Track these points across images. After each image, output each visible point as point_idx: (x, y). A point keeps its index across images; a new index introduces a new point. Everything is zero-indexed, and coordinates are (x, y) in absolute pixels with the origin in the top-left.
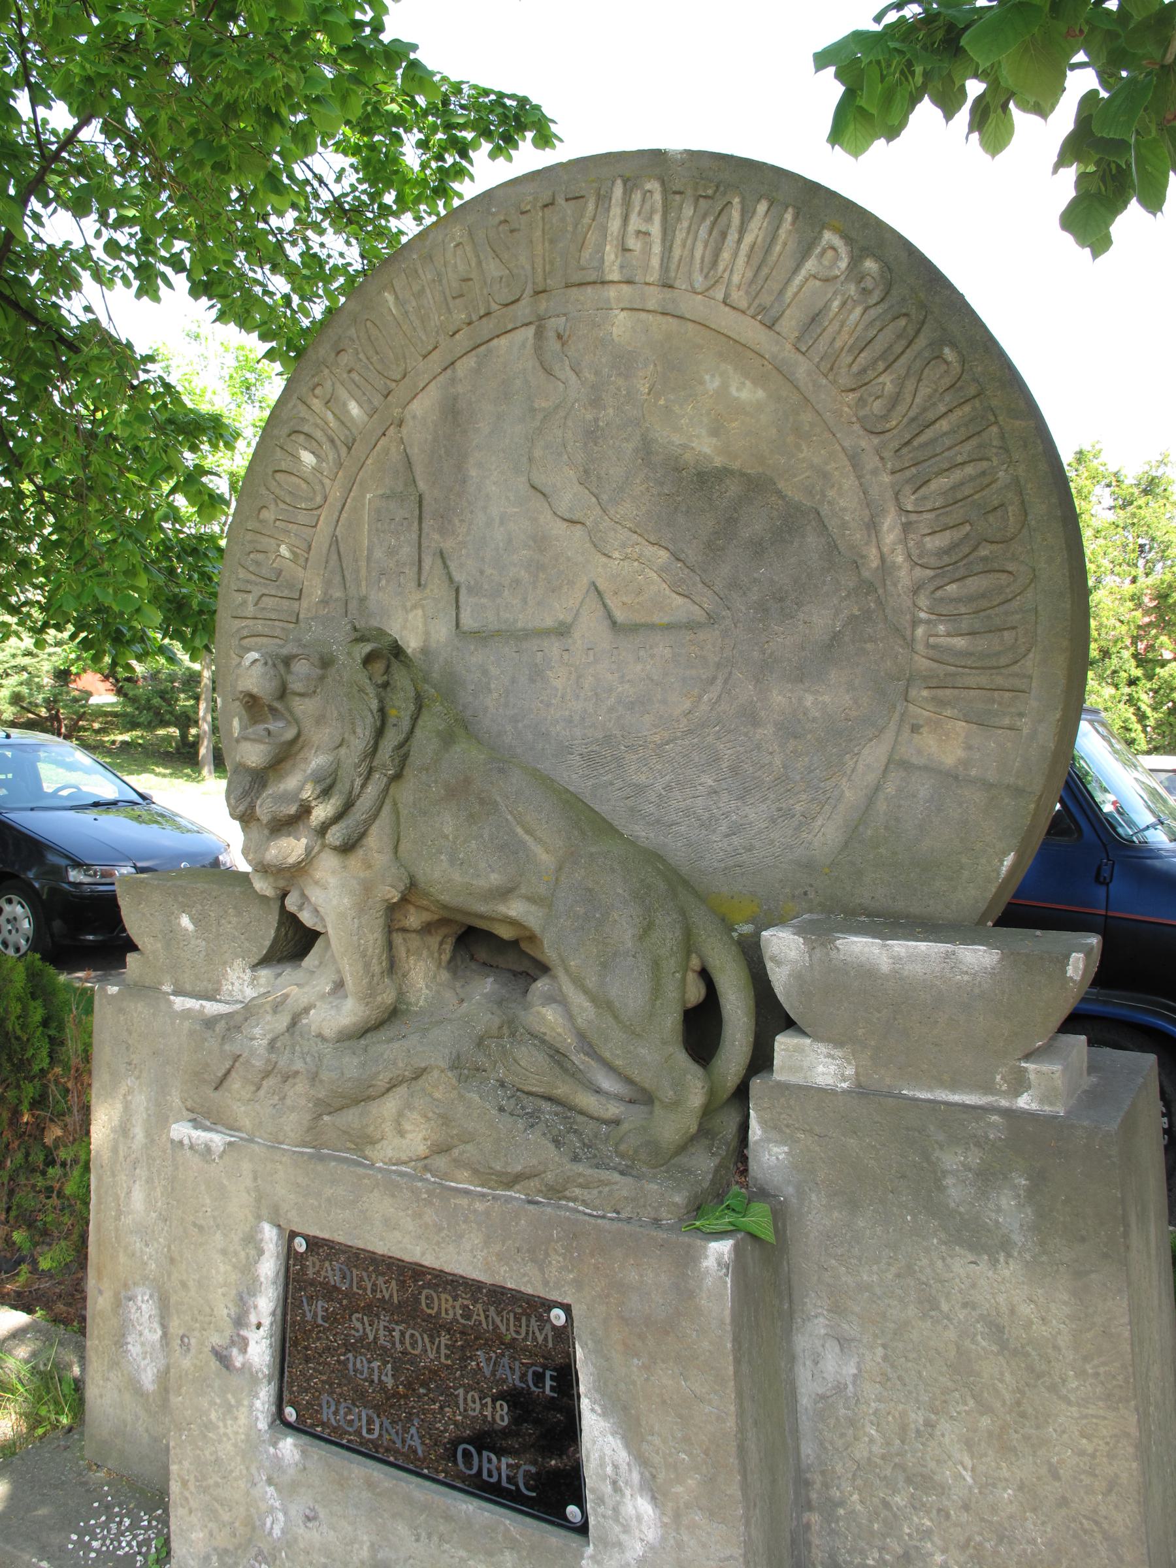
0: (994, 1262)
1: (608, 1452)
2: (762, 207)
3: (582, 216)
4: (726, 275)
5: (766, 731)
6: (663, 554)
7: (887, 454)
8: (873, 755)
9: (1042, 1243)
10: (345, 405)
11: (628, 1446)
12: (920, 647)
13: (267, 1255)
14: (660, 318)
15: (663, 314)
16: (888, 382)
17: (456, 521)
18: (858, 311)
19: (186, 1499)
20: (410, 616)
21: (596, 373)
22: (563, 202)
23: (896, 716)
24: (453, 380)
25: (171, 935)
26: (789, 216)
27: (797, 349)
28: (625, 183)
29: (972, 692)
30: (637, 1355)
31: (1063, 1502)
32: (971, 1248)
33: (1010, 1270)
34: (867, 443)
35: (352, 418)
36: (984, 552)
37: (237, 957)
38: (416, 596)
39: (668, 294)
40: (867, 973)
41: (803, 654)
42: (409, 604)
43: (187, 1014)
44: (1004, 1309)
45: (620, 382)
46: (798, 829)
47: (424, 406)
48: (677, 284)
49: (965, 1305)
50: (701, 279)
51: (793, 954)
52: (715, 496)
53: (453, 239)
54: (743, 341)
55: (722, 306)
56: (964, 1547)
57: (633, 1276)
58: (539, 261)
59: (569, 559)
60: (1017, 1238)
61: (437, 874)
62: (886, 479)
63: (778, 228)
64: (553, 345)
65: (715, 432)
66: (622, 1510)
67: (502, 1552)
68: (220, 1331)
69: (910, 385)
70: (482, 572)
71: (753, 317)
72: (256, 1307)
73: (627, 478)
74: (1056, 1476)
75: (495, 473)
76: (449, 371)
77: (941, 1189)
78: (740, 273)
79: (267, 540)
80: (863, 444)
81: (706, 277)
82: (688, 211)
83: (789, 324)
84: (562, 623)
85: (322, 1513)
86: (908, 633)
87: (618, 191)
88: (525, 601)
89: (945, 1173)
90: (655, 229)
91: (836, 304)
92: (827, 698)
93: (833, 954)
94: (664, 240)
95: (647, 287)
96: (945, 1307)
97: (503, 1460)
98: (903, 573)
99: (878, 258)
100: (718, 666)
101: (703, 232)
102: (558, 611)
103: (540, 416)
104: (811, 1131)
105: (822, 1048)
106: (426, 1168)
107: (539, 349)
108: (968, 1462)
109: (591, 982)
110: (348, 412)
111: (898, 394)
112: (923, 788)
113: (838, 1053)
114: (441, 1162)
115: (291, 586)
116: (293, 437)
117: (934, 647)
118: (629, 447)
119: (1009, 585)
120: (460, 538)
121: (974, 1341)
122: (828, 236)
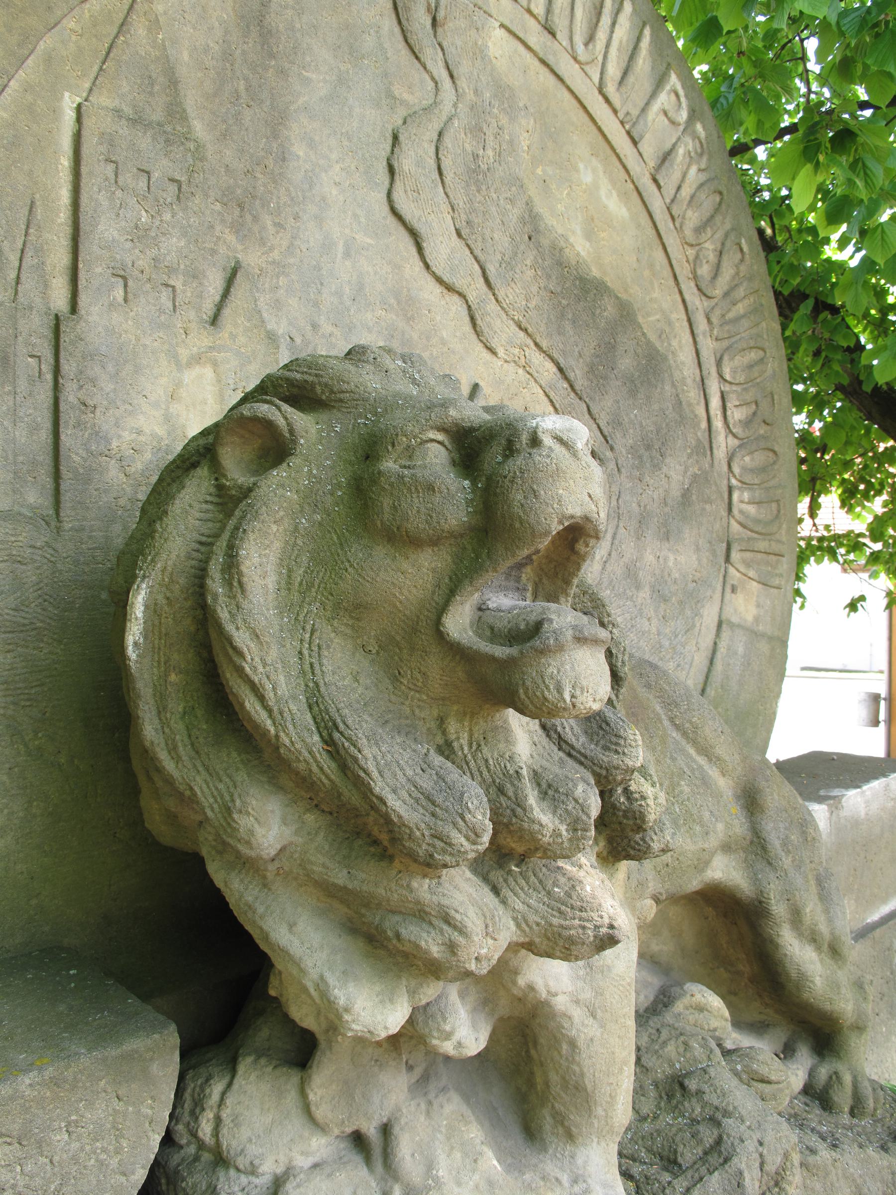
4: (600, 58)
5: (644, 594)
7: (714, 320)
8: (709, 615)
12: (735, 511)
14: (537, 63)
15: (543, 62)
17: (268, 221)
18: (693, 170)
20: (188, 376)
21: (476, 91)
23: (721, 579)
27: (655, 181)
29: (759, 556)
38: (200, 340)
41: (667, 509)
42: (184, 353)
45: (504, 121)
48: (559, 35)
50: (582, 47)
52: (598, 311)
54: (613, 143)
55: (596, 92)
59: (443, 342)
63: (639, 39)
65: (589, 235)
70: (315, 327)
71: (622, 123)
75: (337, 168)
83: (648, 147)
103: (402, 112)
118: (515, 213)
119: (774, 463)
120: (275, 255)
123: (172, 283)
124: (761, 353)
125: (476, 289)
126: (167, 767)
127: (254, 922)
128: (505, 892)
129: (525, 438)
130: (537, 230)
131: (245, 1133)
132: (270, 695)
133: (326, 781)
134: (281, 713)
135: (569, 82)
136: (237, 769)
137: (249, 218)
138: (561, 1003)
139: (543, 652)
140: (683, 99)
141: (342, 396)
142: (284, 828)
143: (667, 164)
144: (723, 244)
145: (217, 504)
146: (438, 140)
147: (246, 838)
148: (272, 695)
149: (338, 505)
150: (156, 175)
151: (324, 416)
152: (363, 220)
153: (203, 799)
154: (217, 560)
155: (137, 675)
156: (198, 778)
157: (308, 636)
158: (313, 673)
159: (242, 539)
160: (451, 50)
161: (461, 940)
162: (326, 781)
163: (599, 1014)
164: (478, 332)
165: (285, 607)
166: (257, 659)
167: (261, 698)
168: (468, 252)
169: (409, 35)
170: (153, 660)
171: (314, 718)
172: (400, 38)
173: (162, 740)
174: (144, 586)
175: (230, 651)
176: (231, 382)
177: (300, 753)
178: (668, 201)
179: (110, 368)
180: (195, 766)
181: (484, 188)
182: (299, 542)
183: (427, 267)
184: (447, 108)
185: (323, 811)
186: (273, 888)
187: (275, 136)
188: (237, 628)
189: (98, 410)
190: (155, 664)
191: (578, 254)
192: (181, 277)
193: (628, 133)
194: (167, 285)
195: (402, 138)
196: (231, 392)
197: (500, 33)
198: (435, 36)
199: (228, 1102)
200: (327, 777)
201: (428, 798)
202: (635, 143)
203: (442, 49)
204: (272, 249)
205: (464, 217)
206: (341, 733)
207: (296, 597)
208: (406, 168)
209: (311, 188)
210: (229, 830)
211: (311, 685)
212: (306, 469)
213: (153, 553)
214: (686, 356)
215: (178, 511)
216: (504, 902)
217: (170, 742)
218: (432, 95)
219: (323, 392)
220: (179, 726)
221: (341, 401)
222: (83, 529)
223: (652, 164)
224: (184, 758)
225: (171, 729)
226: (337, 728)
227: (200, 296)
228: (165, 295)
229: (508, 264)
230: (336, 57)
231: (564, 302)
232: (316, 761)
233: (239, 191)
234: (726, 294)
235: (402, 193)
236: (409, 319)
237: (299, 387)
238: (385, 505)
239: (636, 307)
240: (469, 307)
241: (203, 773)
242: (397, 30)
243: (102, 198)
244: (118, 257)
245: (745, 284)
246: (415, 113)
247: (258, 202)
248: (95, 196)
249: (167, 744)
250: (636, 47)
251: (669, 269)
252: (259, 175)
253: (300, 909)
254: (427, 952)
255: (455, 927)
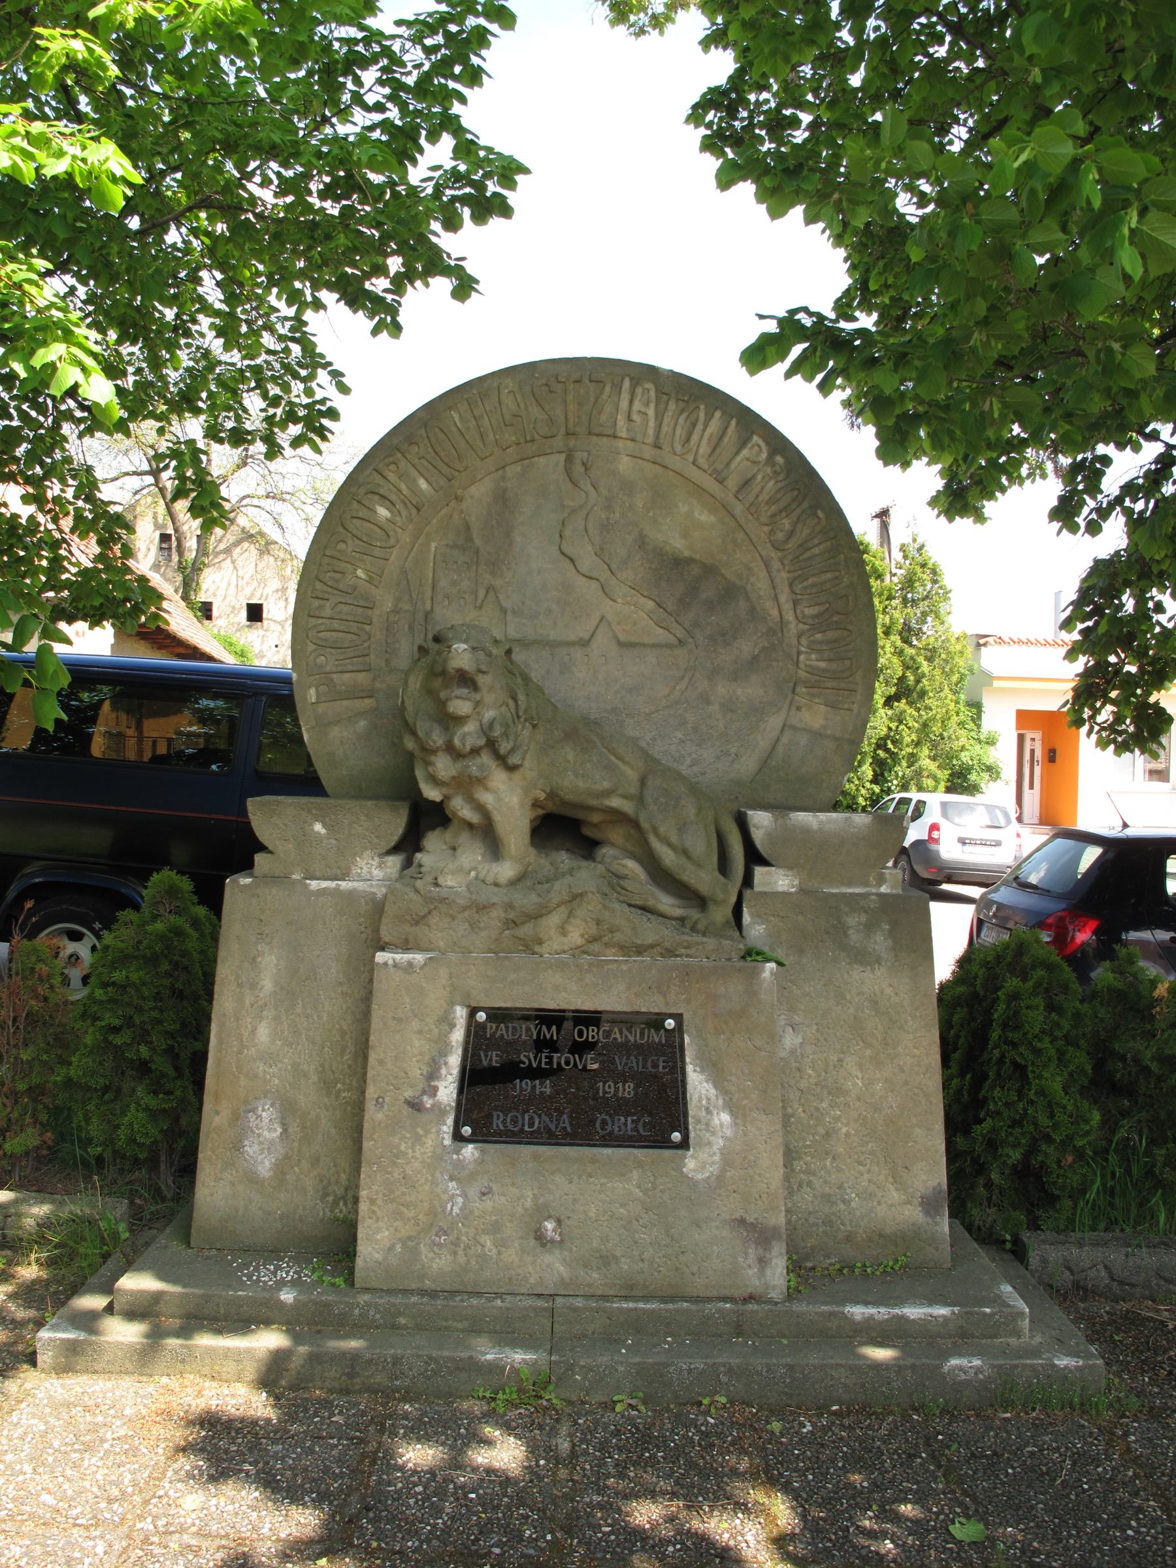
0: (873, 970)
1: (704, 1092)
2: (718, 414)
3: (601, 394)
6: (651, 604)
7: (786, 562)
8: (774, 723)
9: (896, 956)
10: (415, 480)
11: (716, 1087)
12: (802, 665)
13: (458, 1026)
16: (786, 524)
18: (772, 483)
19: (374, 1212)
22: (587, 382)
23: (788, 702)
24: (503, 478)
25: (305, 839)
26: (733, 422)
28: (632, 379)
30: (724, 1033)
31: (906, 1083)
32: (862, 963)
33: (880, 972)
34: (774, 555)
35: (421, 490)
36: (835, 618)
37: (366, 849)
39: (658, 452)
40: (806, 830)
43: (323, 892)
44: (878, 992)
46: (733, 762)
47: (480, 491)
49: (859, 994)
51: (766, 823)
53: (507, 387)
56: (856, 1121)
57: (722, 990)
58: (570, 416)
60: (884, 955)
61: (566, 783)
62: (784, 575)
63: (726, 428)
64: (578, 469)
65: (685, 536)
66: (712, 1123)
67: (631, 1171)
68: (412, 1086)
69: (799, 526)
70: (523, 603)
72: (446, 1064)
74: (902, 1071)
76: (500, 472)
77: (846, 936)
78: (704, 449)
79: (343, 564)
80: (773, 555)
81: (683, 446)
82: (672, 406)
83: (732, 482)
84: (581, 639)
85: (495, 1188)
86: (795, 658)
87: (627, 384)
88: (555, 624)
89: (849, 928)
90: (651, 412)
91: (760, 476)
92: (750, 691)
93: (788, 822)
94: (656, 419)
96: (848, 997)
97: (629, 1119)
98: (792, 626)
99: (783, 456)
100: (686, 670)
101: (681, 420)
102: (581, 631)
104: (778, 916)
105: (781, 871)
106: (584, 952)
107: (568, 470)
108: (860, 1076)
109: (674, 839)
110: (418, 485)
111: (793, 531)
112: (803, 740)
113: (790, 873)
114: (595, 947)
115: (367, 599)
116: (369, 496)
117: (810, 666)
121: (863, 1012)
122: (756, 439)
125: (605, 575)
164: (606, 594)
223: (735, 489)
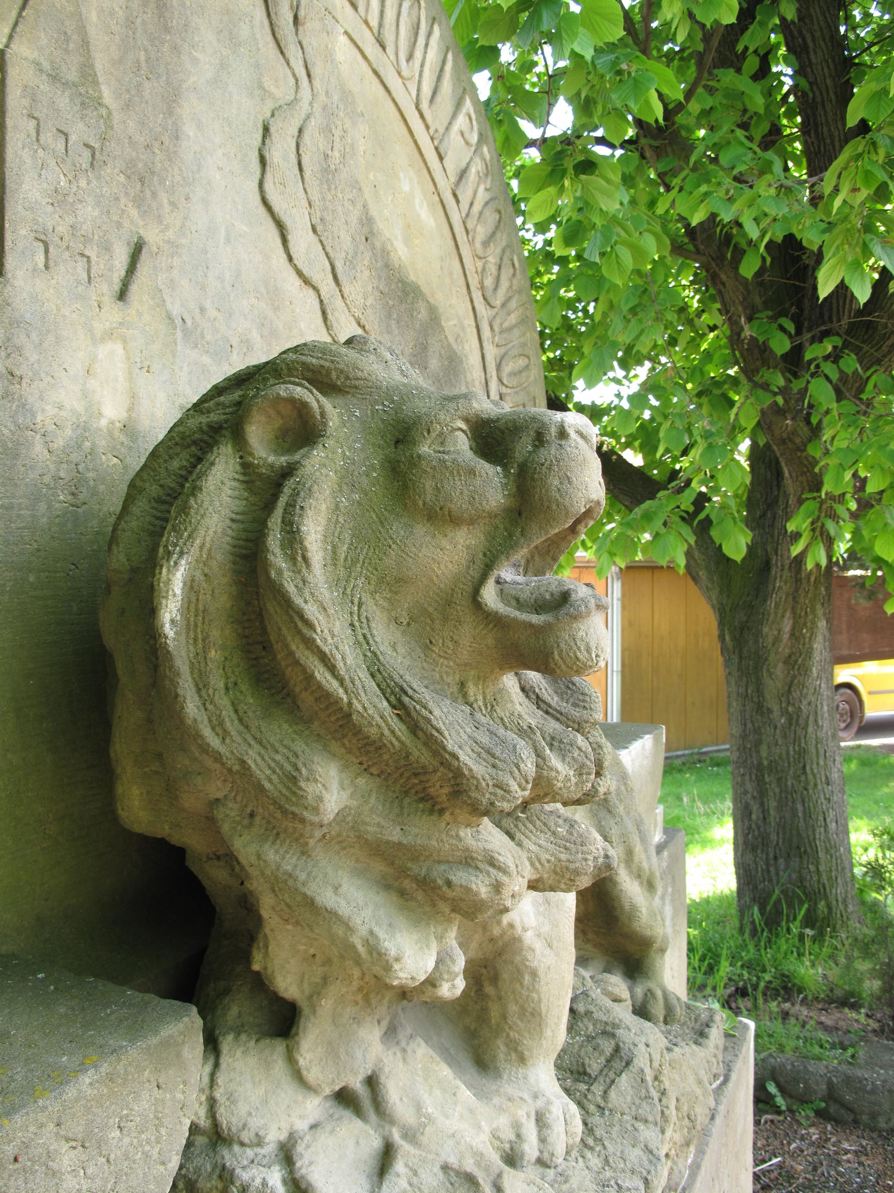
4: (417, 75)
7: (496, 328)
14: (370, 73)
15: (376, 73)
17: (164, 197)
20: (103, 351)
26: (450, 56)
27: (455, 195)
38: (113, 313)
54: (426, 156)
63: (444, 62)
65: (407, 241)
70: (202, 310)
73: (356, 253)
83: (453, 164)
95: (364, 26)
103: (269, 106)
118: (356, 213)
120: (170, 234)
123: (87, 253)
124: (526, 360)
125: (327, 286)
126: (212, 744)
127: (296, 889)
128: (518, 835)
129: (553, 431)
130: (371, 232)
131: (242, 1108)
132: (340, 665)
133: (396, 743)
134: (353, 682)
135: (394, 95)
136: (293, 741)
137: (148, 193)
138: (529, 938)
139: (577, 617)
140: (474, 123)
141: (357, 383)
142: (342, 793)
143: (464, 181)
144: (501, 259)
145: (243, 481)
146: (299, 136)
147: (315, 804)
148: (342, 664)
149: (374, 486)
150: (73, 138)
151: (340, 400)
152: (240, 207)
153: (258, 772)
154: (275, 535)
155: (175, 653)
156: (250, 752)
157: (356, 608)
158: (368, 644)
159: (301, 516)
160: (308, 50)
161: (504, 879)
162: (396, 743)
163: (555, 944)
165: (335, 583)
166: (326, 631)
167: (332, 669)
168: (320, 248)
169: (276, 29)
170: (188, 637)
171: (378, 685)
172: (268, 30)
173: (206, 718)
174: (183, 562)
175: (300, 624)
176: (138, 360)
177: (373, 718)
178: (464, 215)
179: (34, 336)
180: (245, 740)
181: (333, 187)
182: (341, 520)
183: (290, 259)
184: (304, 107)
185: (372, 774)
186: (314, 854)
187: (170, 112)
188: (306, 602)
189: (24, 381)
190: (191, 641)
191: (400, 258)
192: (95, 247)
193: (436, 149)
194: (82, 255)
195: (272, 130)
196: (137, 371)
197: (343, 39)
198: (297, 34)
199: (220, 1081)
200: (397, 738)
201: (489, 752)
202: (441, 158)
203: (302, 48)
204: (167, 228)
205: (318, 213)
206: (411, 697)
207: (342, 572)
208: (275, 160)
209: (199, 170)
210: (294, 799)
211: (369, 654)
212: (340, 451)
213: (189, 529)
214: (474, 359)
215: (212, 488)
216: (520, 845)
217: (214, 719)
218: (293, 91)
219: (338, 378)
220: (224, 702)
221: (356, 387)
222: (12, 507)
224: (233, 733)
225: (215, 705)
226: (406, 693)
227: (111, 269)
228: (81, 264)
229: (350, 262)
230: (219, 41)
231: (391, 302)
232: (388, 725)
233: (140, 165)
234: (504, 305)
235: (271, 185)
236: (276, 309)
237: (313, 371)
238: (427, 487)
239: (441, 310)
240: (321, 301)
241: (257, 747)
242: (266, 22)
243: (26, 155)
244: (40, 220)
245: (516, 296)
246: (280, 106)
247: (156, 178)
248: (19, 152)
249: (210, 721)
250: (442, 70)
251: (463, 278)
252: (156, 151)
253: (340, 872)
254: (477, 894)
255: (499, 868)
